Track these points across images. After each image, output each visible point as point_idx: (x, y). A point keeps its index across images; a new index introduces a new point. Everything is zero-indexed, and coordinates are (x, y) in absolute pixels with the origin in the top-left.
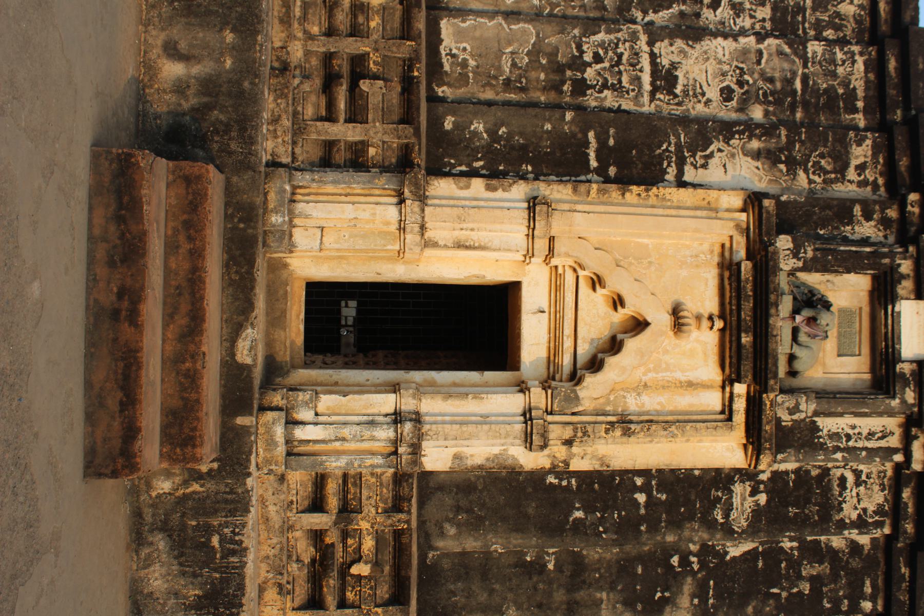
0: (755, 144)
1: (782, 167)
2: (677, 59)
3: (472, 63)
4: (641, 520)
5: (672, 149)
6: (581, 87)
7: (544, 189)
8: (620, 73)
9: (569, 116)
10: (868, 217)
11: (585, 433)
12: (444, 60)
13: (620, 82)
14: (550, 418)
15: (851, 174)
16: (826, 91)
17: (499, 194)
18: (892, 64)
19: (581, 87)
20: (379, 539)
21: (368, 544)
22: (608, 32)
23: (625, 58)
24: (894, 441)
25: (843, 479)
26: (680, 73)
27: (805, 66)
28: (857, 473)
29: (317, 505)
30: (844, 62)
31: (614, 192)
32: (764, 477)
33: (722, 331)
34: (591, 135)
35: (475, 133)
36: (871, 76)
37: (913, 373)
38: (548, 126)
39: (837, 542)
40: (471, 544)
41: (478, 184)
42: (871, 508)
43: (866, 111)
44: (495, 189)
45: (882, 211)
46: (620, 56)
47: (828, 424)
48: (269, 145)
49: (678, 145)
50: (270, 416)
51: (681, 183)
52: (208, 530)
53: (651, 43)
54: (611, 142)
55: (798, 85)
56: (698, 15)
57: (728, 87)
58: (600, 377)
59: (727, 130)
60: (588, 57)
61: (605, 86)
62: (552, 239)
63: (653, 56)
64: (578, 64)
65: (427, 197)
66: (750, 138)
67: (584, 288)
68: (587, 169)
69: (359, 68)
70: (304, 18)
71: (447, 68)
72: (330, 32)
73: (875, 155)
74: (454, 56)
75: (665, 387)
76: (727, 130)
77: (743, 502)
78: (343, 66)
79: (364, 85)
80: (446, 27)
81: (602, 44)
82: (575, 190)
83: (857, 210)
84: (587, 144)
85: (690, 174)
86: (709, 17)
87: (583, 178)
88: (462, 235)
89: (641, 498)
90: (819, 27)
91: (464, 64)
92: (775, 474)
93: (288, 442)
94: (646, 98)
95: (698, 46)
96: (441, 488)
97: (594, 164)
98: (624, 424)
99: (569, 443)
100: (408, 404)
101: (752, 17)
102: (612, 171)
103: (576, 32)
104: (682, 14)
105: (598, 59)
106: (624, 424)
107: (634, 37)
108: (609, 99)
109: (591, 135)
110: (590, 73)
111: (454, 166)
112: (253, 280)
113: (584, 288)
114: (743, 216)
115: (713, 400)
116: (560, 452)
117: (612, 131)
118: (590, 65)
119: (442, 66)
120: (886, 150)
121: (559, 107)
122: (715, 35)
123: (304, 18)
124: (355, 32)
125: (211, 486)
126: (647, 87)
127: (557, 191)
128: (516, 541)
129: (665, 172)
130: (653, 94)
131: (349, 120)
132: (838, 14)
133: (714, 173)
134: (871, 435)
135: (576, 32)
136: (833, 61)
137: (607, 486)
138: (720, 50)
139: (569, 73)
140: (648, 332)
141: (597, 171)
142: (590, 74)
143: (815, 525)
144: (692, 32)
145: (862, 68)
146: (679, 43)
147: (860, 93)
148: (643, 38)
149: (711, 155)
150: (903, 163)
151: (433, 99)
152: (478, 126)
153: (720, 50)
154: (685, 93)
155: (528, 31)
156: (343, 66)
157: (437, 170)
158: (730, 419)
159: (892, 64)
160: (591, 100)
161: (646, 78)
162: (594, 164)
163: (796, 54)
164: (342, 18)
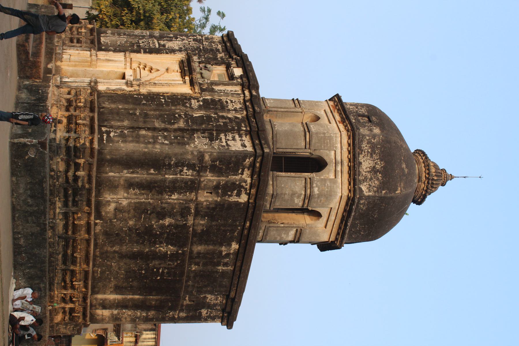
4: (164, 104)
24: (240, 92)
25: (227, 102)
28: (232, 102)
29: (69, 93)
32: (201, 99)
33: (181, 72)
39: (230, 116)
40: (113, 106)
41: (111, 53)
42: (238, 108)
47: (216, 88)
52: (39, 90)
62: (131, 59)
67: (142, 70)
77: (195, 104)
88: (108, 58)
89: (163, 100)
92: (204, 99)
93: (61, 82)
96: (104, 96)
99: (139, 85)
112: (52, 58)
113: (142, 70)
116: (137, 88)
125: (40, 84)
128: (126, 106)
134: (231, 91)
137: (153, 97)
143: (220, 110)
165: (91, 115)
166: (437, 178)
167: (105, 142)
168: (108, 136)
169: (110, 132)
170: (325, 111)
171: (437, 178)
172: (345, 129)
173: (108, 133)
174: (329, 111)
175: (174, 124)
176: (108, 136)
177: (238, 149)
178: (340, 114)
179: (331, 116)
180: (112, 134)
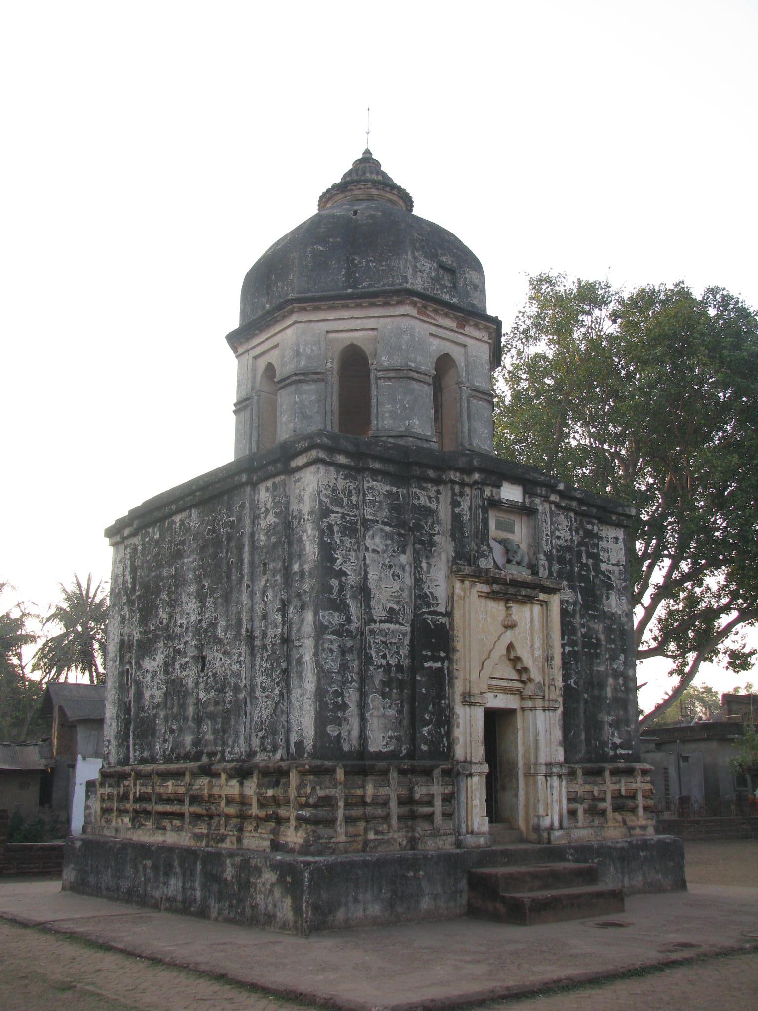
0: (424, 565)
1: (434, 549)
2: (381, 607)
3: (390, 733)
5: (430, 617)
6: (399, 668)
7: (458, 698)
8: (391, 643)
9: (418, 678)
10: (459, 505)
11: (553, 680)
12: (389, 749)
13: (395, 644)
14: (546, 697)
15: (433, 506)
16: (390, 511)
17: (461, 720)
18: (377, 465)
19: (399, 668)
20: (585, 783)
21: (588, 788)
22: (370, 648)
23: (384, 639)
26: (389, 605)
27: (377, 522)
30: (373, 495)
31: (455, 656)
34: (427, 665)
35: (429, 732)
36: (379, 478)
37: (529, 497)
38: (424, 690)
43: (398, 487)
44: (459, 724)
45: (456, 495)
46: (383, 642)
48: (447, 847)
49: (430, 613)
50: (552, 838)
51: (449, 614)
53: (375, 622)
54: (429, 653)
55: (388, 529)
56: (352, 587)
57: (393, 575)
58: (531, 670)
59: (418, 582)
60: (384, 662)
61: (397, 653)
63: (381, 622)
64: (388, 668)
65: (465, 761)
66: (421, 568)
68: (441, 670)
69: (407, 801)
70: (382, 833)
71: (392, 748)
72: (387, 818)
73: (424, 489)
74: (387, 744)
75: (532, 635)
76: (418, 582)
78: (405, 810)
79: (417, 796)
80: (372, 749)
81: (377, 653)
82: (456, 678)
83: (457, 510)
84: (431, 668)
85: (441, 609)
86: (352, 579)
87: (446, 672)
90: (355, 506)
91: (391, 737)
94: (402, 628)
95: (373, 591)
97: (439, 665)
98: (549, 659)
100: (543, 769)
101: (350, 551)
102: (442, 654)
103: (371, 668)
104: (351, 597)
105: (384, 656)
106: (549, 659)
107: (372, 632)
108: (404, 651)
109: (427, 665)
110: (393, 662)
111: (444, 746)
114: (467, 582)
115: (537, 608)
117: (424, 653)
118: (388, 661)
119: (392, 751)
120: (423, 480)
121: (413, 681)
122: (365, 578)
123: (382, 833)
124: (386, 804)
126: (397, 626)
127: (459, 687)
129: (441, 623)
130: (401, 624)
131: (433, 806)
132: (343, 490)
133: (441, 593)
135: (371, 668)
136: (374, 502)
138: (375, 577)
139: (393, 675)
140: (514, 643)
141: (443, 663)
142: (393, 662)
144: (364, 592)
145: (375, 483)
146: (372, 603)
147: (388, 488)
148: (372, 626)
149: (431, 593)
150: (431, 474)
151: (411, 755)
152: (425, 731)
153: (375, 577)
154: (398, 603)
155: (375, 701)
156: (405, 810)
157: (448, 754)
158: (546, 602)
159: (377, 465)
160: (406, 663)
161: (392, 626)
162: (439, 665)
163: (372, 527)
164: (379, 811)
165: (607, 774)
166: (367, 178)
167: (630, 752)
168: (621, 746)
169: (614, 744)
170: (431, 334)
171: (367, 178)
172: (479, 329)
173: (615, 747)
174: (434, 328)
175: (598, 639)
176: (621, 746)
177: (623, 552)
178: (446, 315)
179: (448, 333)
180: (618, 741)
